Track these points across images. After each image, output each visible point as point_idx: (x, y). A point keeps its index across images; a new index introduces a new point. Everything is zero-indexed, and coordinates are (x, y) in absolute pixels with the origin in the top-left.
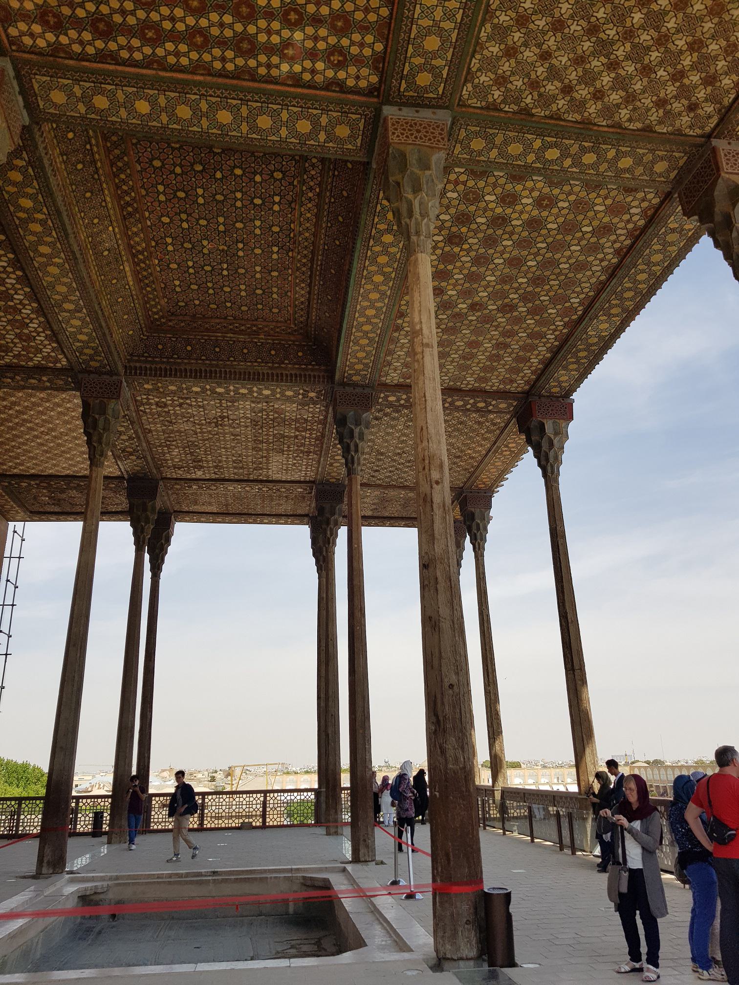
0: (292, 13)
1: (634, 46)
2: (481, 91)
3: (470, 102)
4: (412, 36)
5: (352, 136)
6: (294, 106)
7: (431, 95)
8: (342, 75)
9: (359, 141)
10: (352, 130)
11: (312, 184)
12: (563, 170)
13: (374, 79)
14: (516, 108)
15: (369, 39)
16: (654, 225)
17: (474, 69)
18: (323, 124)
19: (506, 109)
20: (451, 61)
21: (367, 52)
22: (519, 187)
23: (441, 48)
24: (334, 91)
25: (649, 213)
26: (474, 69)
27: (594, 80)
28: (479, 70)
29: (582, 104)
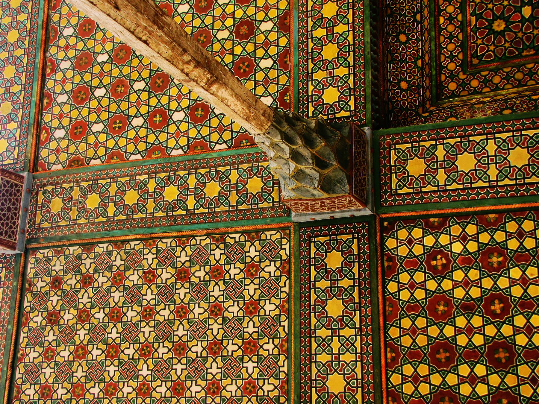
0: (498, 311)
1: (136, 340)
2: (269, 251)
3: (278, 235)
4: (357, 313)
5: (403, 163)
6: (482, 188)
7: (322, 239)
8: (429, 241)
9: (394, 157)
10: (405, 171)
11: (451, 28)
12: (153, 173)
13: (391, 243)
14: (228, 240)
15: (405, 295)
16: (32, 121)
17: (284, 278)
18: (441, 171)
19: (237, 236)
20: (310, 289)
21: (404, 278)
22: (193, 133)
23: (324, 303)
24: (434, 216)
25: (44, 136)
26: (284, 278)
27: (159, 293)
28: (278, 279)
29: (162, 263)
